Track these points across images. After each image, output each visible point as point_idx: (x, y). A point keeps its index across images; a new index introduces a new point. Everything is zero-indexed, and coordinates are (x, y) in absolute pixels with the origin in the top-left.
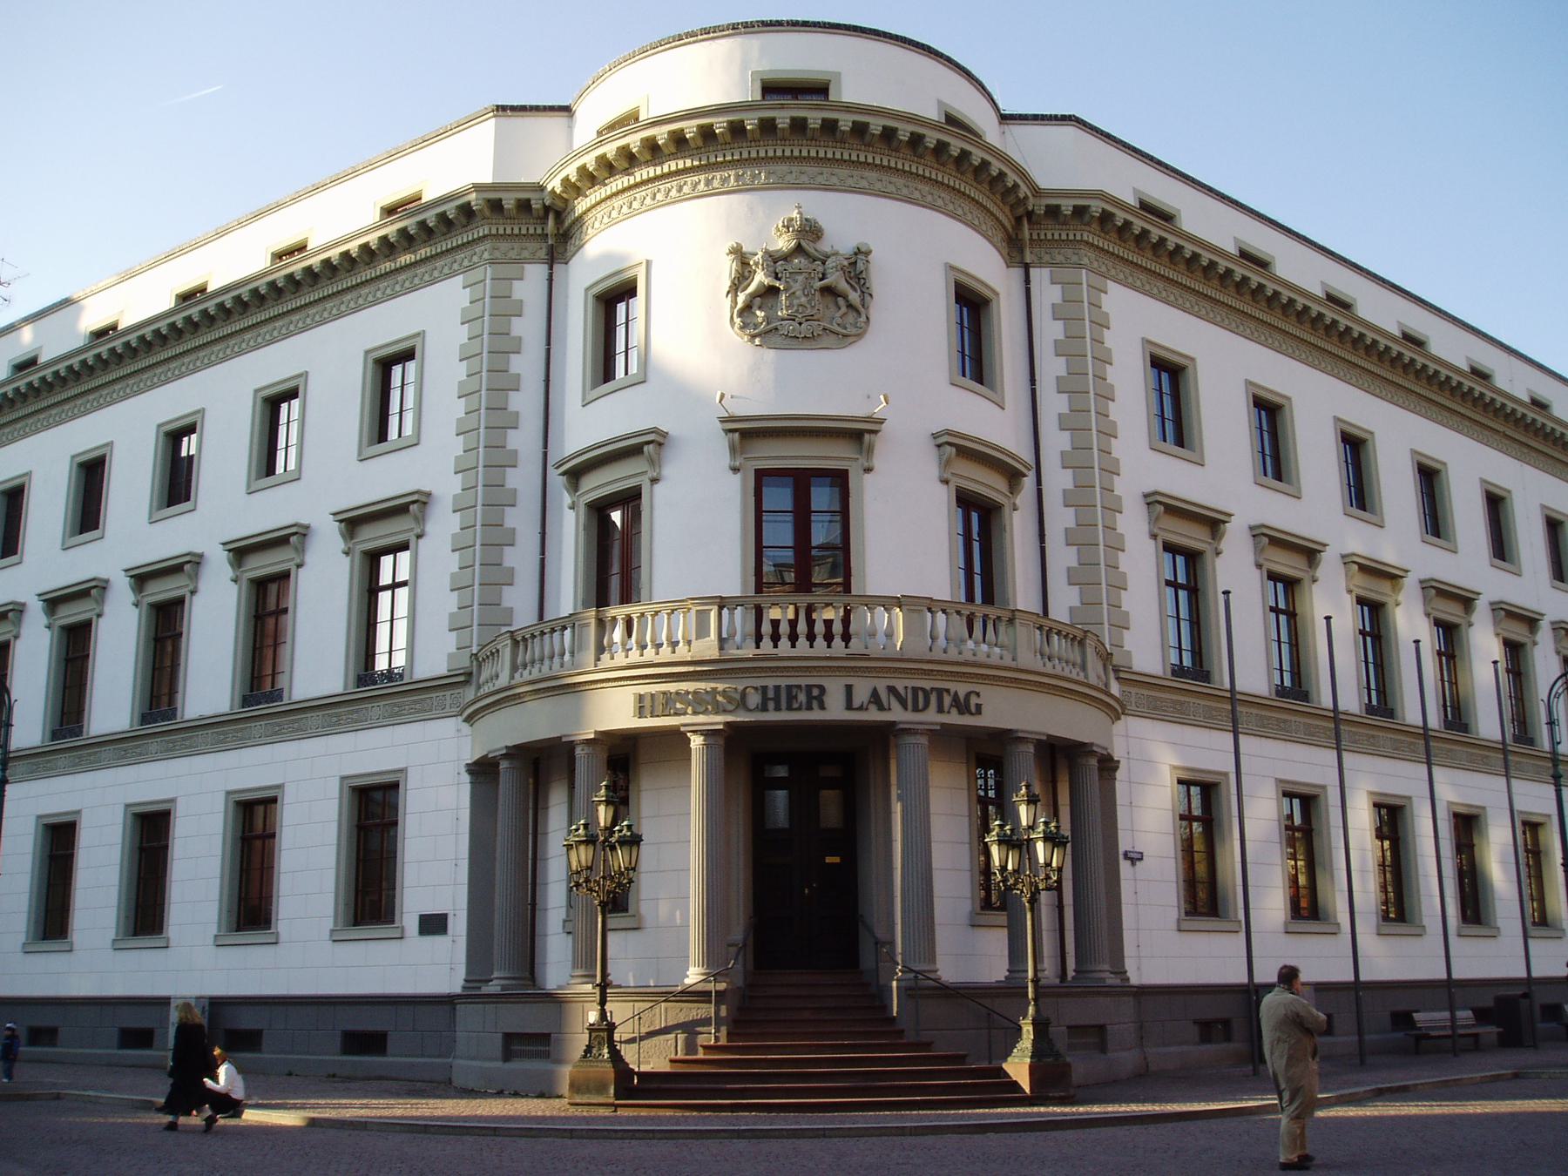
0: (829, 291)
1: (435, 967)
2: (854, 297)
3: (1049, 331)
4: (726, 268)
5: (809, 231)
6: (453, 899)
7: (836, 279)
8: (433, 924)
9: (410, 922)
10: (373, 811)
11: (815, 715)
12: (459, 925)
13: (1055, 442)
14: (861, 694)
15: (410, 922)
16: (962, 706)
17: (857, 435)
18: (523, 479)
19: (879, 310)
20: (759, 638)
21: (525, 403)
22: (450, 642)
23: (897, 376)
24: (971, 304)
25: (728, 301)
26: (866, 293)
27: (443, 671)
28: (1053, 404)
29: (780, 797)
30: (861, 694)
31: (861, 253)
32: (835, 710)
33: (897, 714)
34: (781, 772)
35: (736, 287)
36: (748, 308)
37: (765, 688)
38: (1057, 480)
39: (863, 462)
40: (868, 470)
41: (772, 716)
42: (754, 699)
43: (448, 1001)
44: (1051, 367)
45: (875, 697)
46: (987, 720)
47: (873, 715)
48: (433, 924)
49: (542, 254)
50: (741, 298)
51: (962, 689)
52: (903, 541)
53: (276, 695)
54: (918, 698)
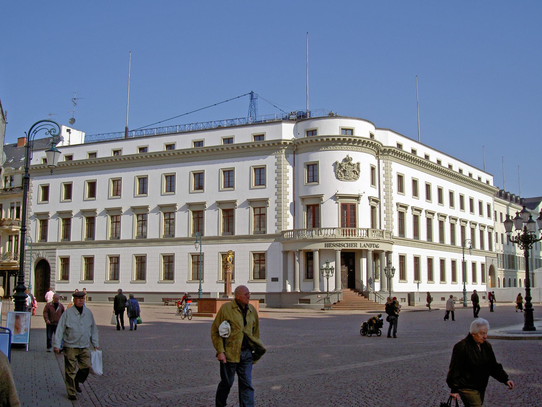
0: (354, 171)
2: (358, 172)
3: (382, 172)
7: (355, 169)
11: (356, 248)
13: (383, 194)
14: (362, 245)
16: (377, 247)
17: (358, 198)
19: (361, 174)
20: (343, 235)
24: (373, 169)
26: (359, 171)
28: (383, 187)
30: (362, 245)
31: (358, 164)
32: (358, 247)
33: (367, 248)
37: (347, 244)
38: (383, 201)
41: (349, 248)
42: (346, 245)
43: (280, 293)
44: (382, 179)
45: (364, 245)
47: (364, 248)
49: (293, 152)
51: (376, 243)
54: (370, 246)
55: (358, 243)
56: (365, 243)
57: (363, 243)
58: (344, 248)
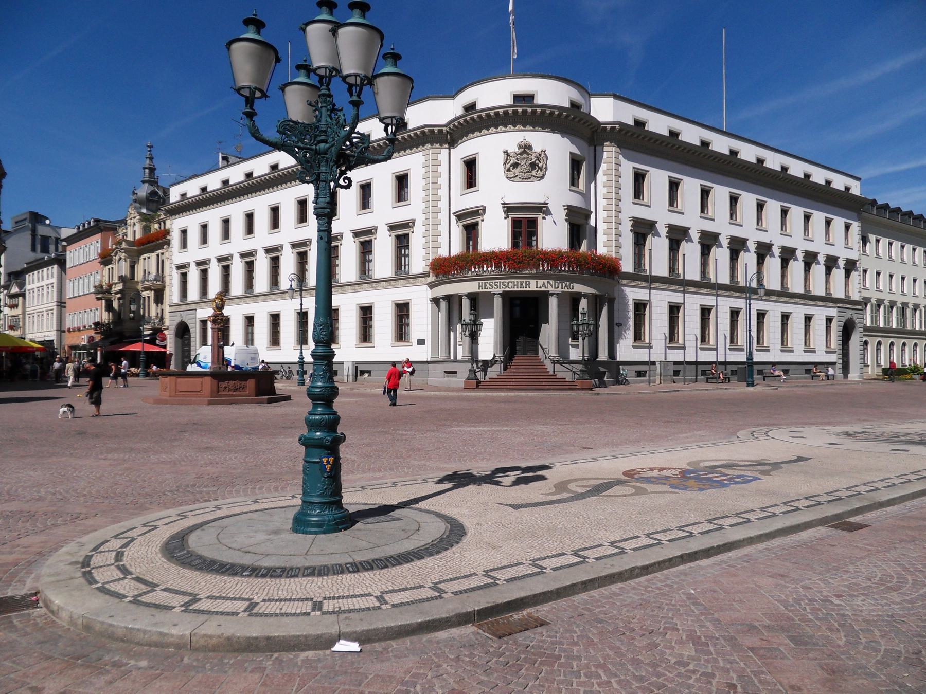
1: (421, 354)
4: (502, 157)
5: (526, 148)
6: (427, 336)
8: (421, 342)
9: (414, 342)
10: (403, 311)
11: (528, 289)
12: (428, 342)
15: (414, 341)
17: (542, 208)
18: (443, 216)
21: (443, 193)
22: (423, 264)
23: (553, 190)
25: (502, 167)
27: (421, 272)
29: (517, 310)
33: (550, 289)
34: (518, 302)
35: (505, 163)
36: (509, 170)
39: (542, 215)
40: (544, 218)
41: (516, 289)
45: (544, 285)
46: (575, 290)
47: (543, 289)
48: (421, 342)
50: (508, 166)
52: (552, 236)
53: (370, 277)
55: (533, 282)
56: (546, 282)
57: (541, 282)
58: (507, 289)
